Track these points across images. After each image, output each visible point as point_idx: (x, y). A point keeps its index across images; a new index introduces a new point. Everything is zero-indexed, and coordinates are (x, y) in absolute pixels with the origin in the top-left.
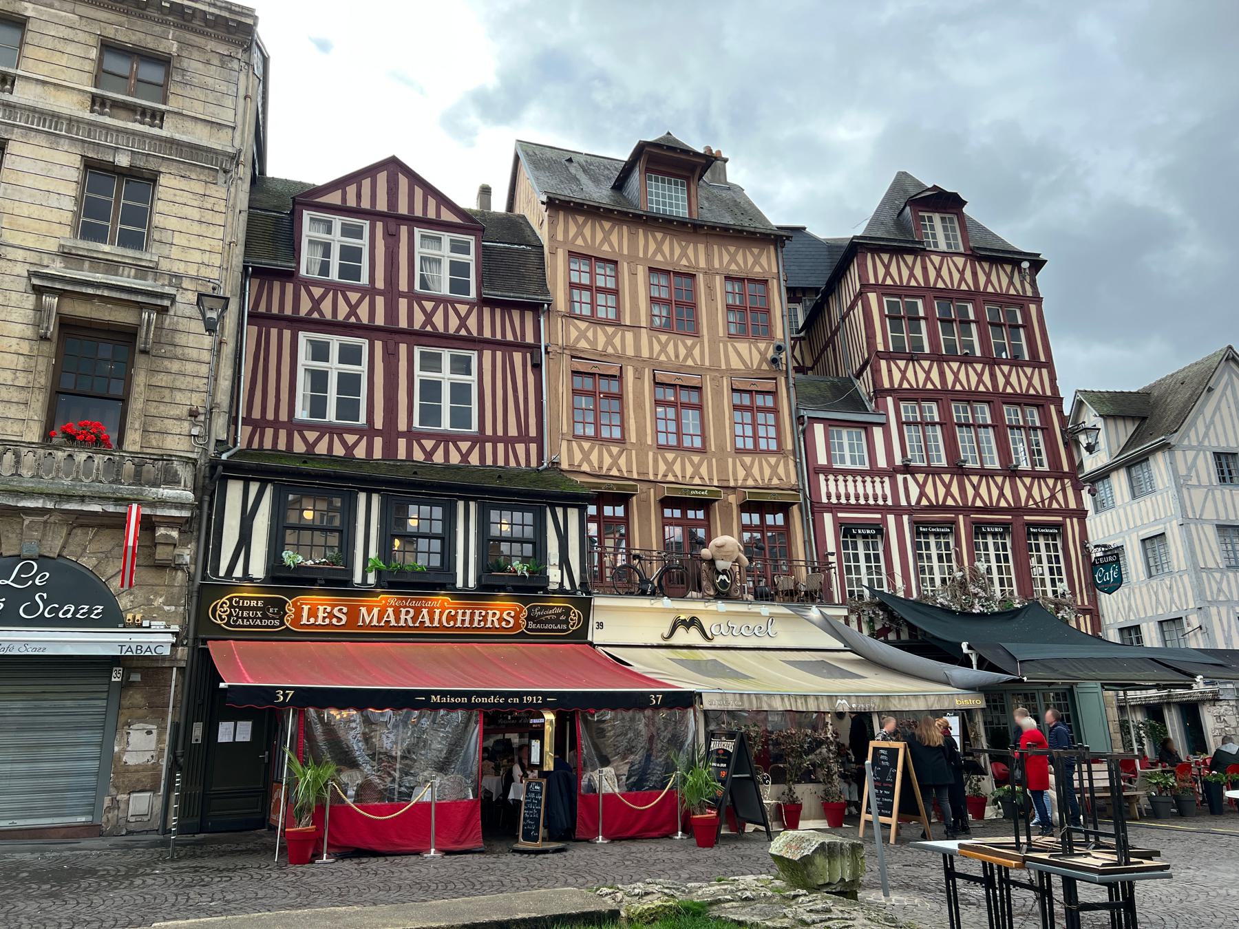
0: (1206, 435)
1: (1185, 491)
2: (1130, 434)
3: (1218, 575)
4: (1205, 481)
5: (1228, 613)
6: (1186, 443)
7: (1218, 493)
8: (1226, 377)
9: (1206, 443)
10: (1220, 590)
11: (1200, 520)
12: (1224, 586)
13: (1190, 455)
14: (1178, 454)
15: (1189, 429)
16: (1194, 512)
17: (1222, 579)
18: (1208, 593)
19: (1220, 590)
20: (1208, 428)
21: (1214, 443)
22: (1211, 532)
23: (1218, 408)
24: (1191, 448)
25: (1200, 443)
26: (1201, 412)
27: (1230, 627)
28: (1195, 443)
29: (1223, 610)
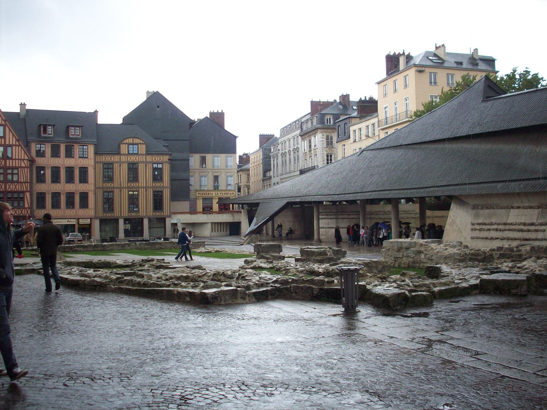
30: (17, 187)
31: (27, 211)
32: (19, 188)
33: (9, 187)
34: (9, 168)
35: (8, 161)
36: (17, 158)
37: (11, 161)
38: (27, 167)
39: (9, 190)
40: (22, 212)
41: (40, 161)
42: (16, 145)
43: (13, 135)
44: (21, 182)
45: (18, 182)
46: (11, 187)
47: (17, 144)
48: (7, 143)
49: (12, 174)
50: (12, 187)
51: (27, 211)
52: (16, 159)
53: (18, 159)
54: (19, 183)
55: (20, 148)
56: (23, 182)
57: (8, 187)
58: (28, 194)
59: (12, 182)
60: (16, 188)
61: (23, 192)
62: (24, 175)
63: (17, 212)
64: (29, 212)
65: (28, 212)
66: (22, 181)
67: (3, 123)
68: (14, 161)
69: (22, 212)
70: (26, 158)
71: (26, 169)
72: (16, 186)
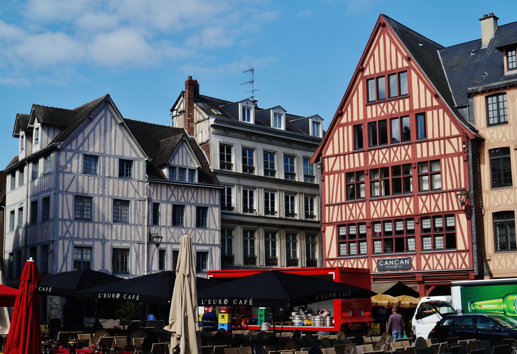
0: (82, 144)
1: (61, 175)
2: (55, 136)
3: (68, 223)
4: (74, 170)
5: (69, 243)
6: (69, 147)
7: (80, 179)
8: (103, 112)
9: (81, 149)
10: (67, 231)
11: (67, 192)
12: (71, 230)
13: (70, 154)
14: (63, 154)
15: (72, 140)
16: (63, 187)
17: (70, 225)
18: (60, 233)
19: (67, 231)
20: (84, 140)
21: (86, 149)
22: (71, 199)
23: (93, 129)
24: (71, 150)
25: (78, 148)
26: (82, 130)
27: (68, 251)
28: (74, 148)
29: (66, 243)
30: (440, 203)
31: (463, 259)
32: (442, 204)
33: (424, 205)
34: (422, 164)
35: (418, 146)
36: (436, 136)
37: (424, 144)
38: (458, 154)
39: (424, 211)
40: (451, 262)
41: (494, 138)
42: (432, 108)
43: (426, 87)
44: (447, 192)
45: (440, 192)
46: (427, 204)
47: (436, 103)
48: (416, 106)
49: (431, 175)
50: (428, 205)
51: (463, 259)
52: (433, 140)
53: (439, 139)
54: (443, 193)
55: (441, 111)
56: (450, 192)
57: (421, 204)
58: (463, 217)
59: (432, 191)
60: (437, 205)
61: (451, 214)
62: (453, 175)
63: (442, 262)
64: (467, 260)
65: (464, 262)
66: (450, 188)
67: (406, 64)
68: (431, 144)
69: (451, 262)
70: (455, 132)
71: (456, 159)
72: (436, 201)
